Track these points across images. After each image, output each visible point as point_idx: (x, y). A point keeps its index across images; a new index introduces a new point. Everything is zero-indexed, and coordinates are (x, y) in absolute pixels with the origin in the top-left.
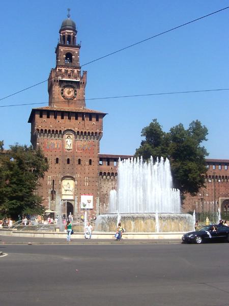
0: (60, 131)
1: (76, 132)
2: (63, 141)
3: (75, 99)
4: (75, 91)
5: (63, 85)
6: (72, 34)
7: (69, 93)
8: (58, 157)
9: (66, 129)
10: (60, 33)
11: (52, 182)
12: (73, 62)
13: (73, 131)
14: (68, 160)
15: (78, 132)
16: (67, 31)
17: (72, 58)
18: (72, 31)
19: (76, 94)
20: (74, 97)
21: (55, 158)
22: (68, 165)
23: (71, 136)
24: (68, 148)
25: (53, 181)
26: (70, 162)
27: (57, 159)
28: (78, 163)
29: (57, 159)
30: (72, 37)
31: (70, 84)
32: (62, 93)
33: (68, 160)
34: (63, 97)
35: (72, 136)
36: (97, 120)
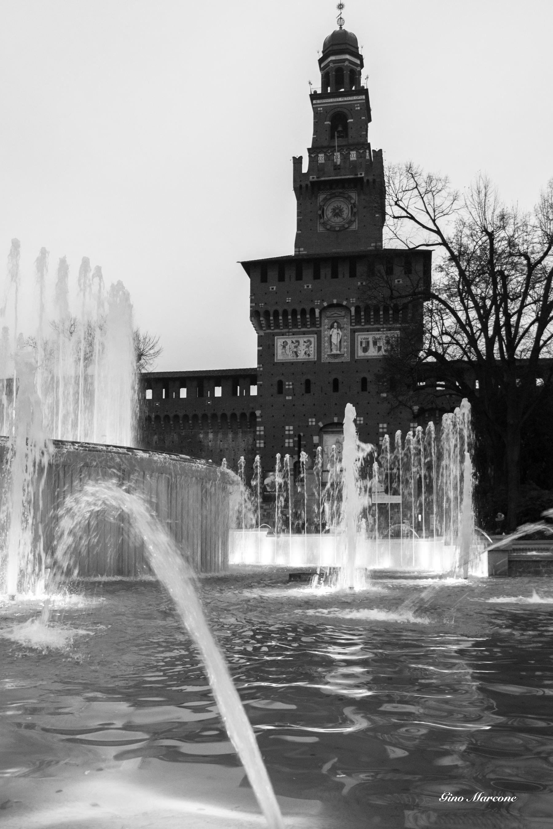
0: (312, 311)
1: (353, 309)
2: (319, 334)
3: (354, 227)
4: (354, 206)
5: (321, 197)
6: (347, 63)
7: (337, 213)
8: (309, 377)
9: (325, 304)
10: (321, 69)
11: (296, 439)
12: (351, 133)
13: (347, 308)
14: (336, 382)
15: (358, 309)
16: (332, 58)
17: (347, 123)
18: (348, 57)
19: (354, 214)
20: (351, 222)
21: (303, 381)
22: (335, 393)
23: (340, 320)
24: (334, 352)
25: (299, 436)
26: (340, 386)
27: (308, 383)
28: (359, 389)
29: (308, 383)
30: (346, 73)
31: (341, 191)
32: (322, 216)
33: (336, 382)
34: (324, 224)
35: (345, 321)
36: (408, 271)
